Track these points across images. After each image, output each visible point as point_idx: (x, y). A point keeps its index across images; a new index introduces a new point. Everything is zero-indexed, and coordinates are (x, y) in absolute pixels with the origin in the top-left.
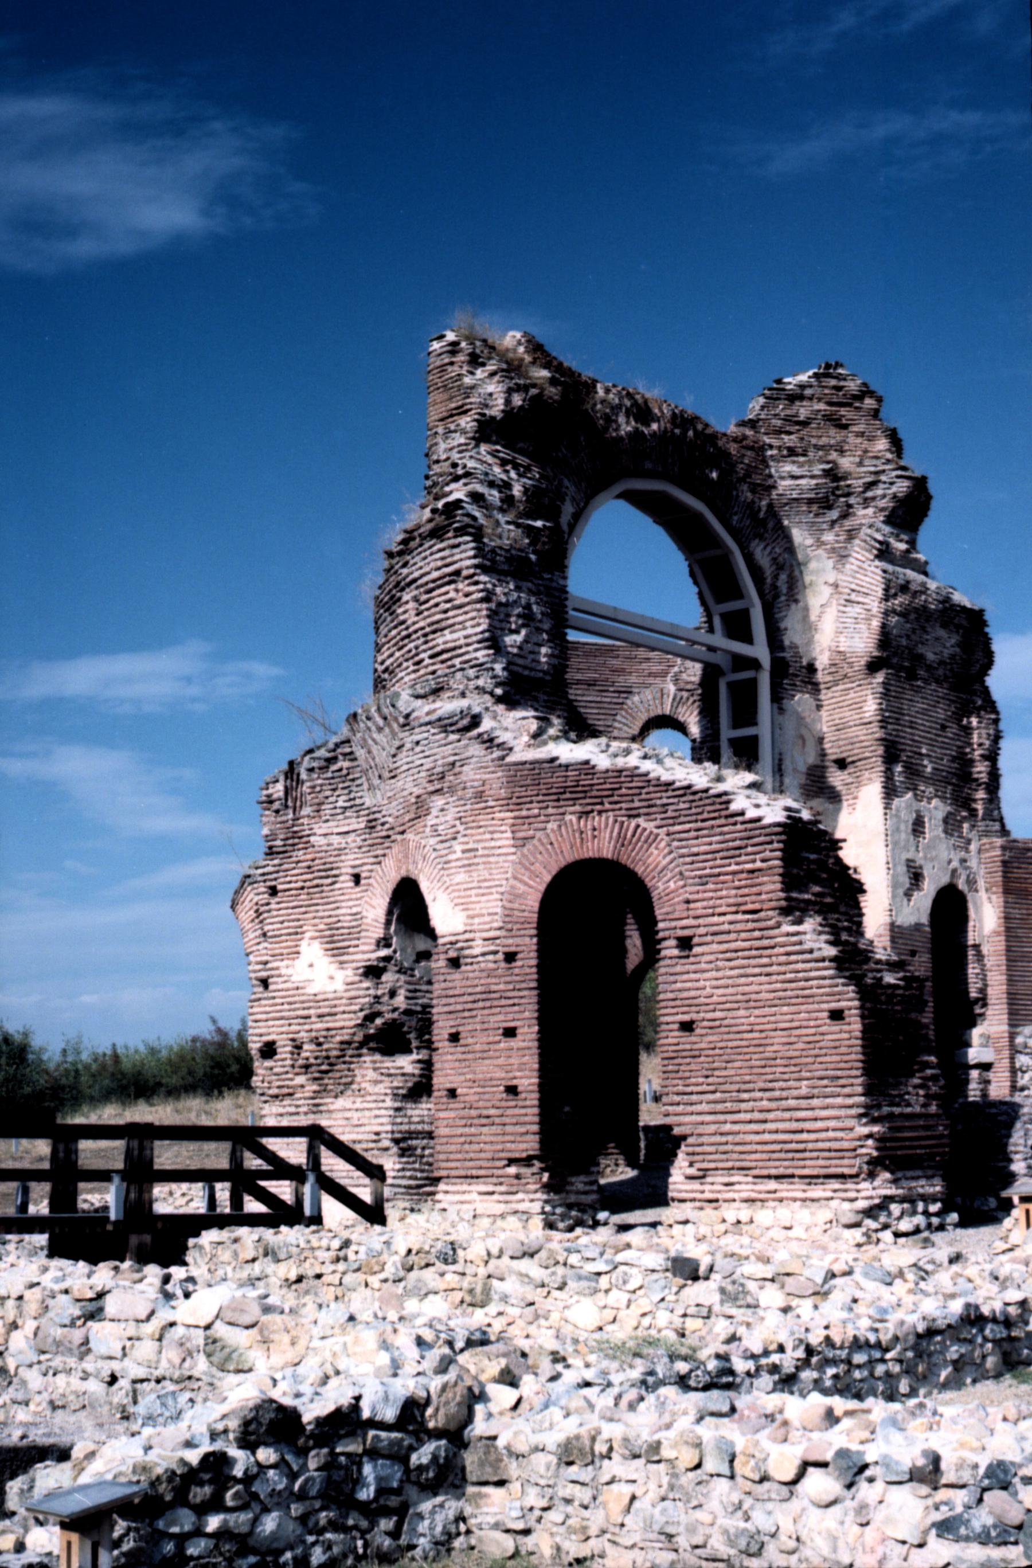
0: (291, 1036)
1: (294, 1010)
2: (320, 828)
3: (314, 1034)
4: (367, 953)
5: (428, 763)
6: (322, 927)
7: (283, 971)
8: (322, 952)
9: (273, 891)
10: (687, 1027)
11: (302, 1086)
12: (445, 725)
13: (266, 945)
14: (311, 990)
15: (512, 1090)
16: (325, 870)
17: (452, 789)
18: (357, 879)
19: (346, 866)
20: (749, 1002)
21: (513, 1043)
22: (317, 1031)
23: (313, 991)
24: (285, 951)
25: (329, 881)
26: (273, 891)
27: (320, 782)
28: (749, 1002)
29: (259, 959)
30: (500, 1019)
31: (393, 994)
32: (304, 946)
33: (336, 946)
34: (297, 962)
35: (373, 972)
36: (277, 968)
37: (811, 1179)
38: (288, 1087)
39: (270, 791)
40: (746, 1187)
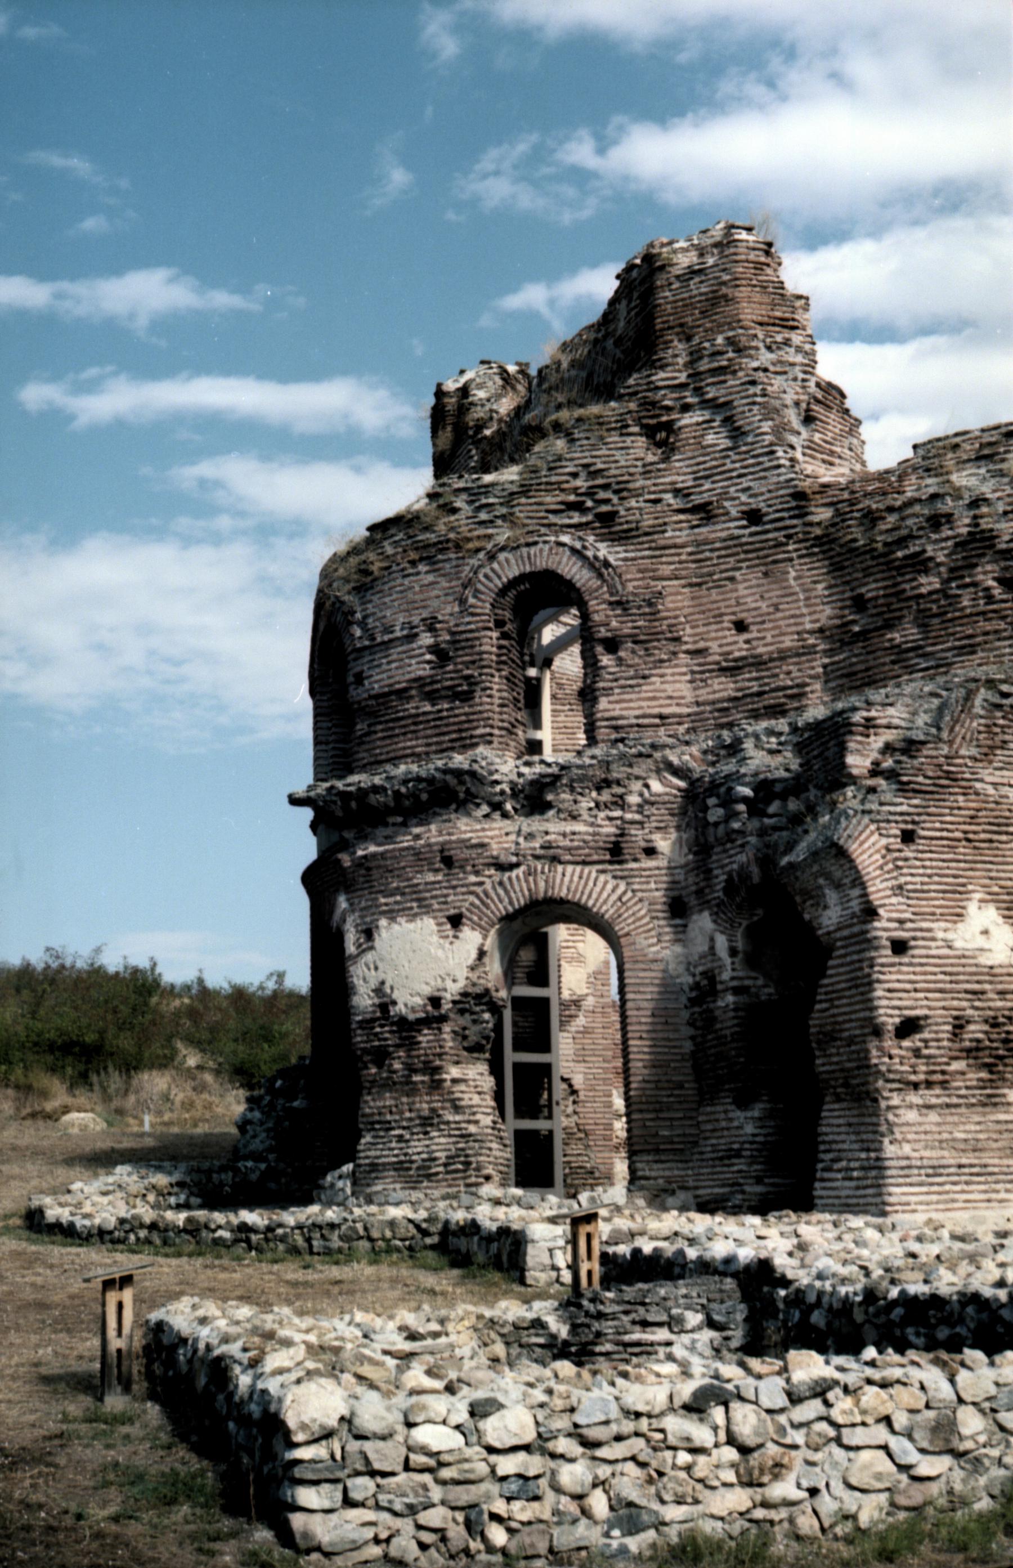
0: (955, 1013)
1: (957, 982)
2: (988, 774)
3: (991, 1013)
6: (996, 889)
7: (940, 935)
8: (1001, 920)
11: (963, 1073)
13: (901, 899)
14: (985, 960)
16: (998, 825)
22: (998, 1009)
23: (989, 963)
24: (938, 911)
25: (1004, 838)
26: (908, 837)
27: (1001, 722)
29: (895, 915)
32: (972, 907)
34: (960, 925)
36: (929, 930)
38: (943, 1072)
39: (873, 713)
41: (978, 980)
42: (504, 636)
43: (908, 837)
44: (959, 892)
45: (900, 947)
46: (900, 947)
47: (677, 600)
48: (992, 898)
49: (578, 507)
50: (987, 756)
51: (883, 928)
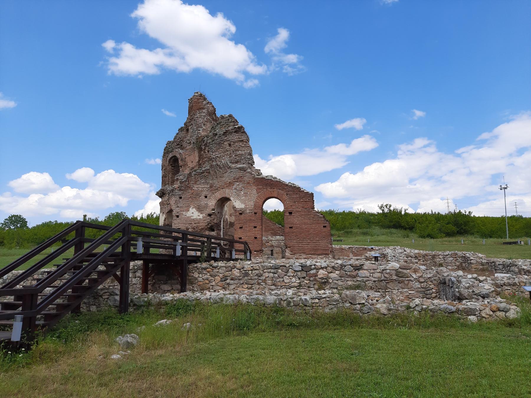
4: (209, 211)
5: (234, 176)
9: (181, 198)
10: (290, 227)
12: (240, 169)
15: (256, 238)
17: (240, 181)
18: (206, 197)
19: (204, 193)
20: (305, 224)
21: (256, 229)
28: (305, 224)
30: (253, 225)
31: (214, 220)
32: (191, 209)
33: (200, 209)
35: (210, 215)
37: (319, 255)
40: (305, 256)
41: (190, 221)
42: (172, 167)
43: (181, 198)
44: (189, 207)
45: (178, 216)
46: (178, 216)
47: (188, 159)
48: (195, 207)
49: (178, 144)
50: (195, 183)
51: (174, 213)
